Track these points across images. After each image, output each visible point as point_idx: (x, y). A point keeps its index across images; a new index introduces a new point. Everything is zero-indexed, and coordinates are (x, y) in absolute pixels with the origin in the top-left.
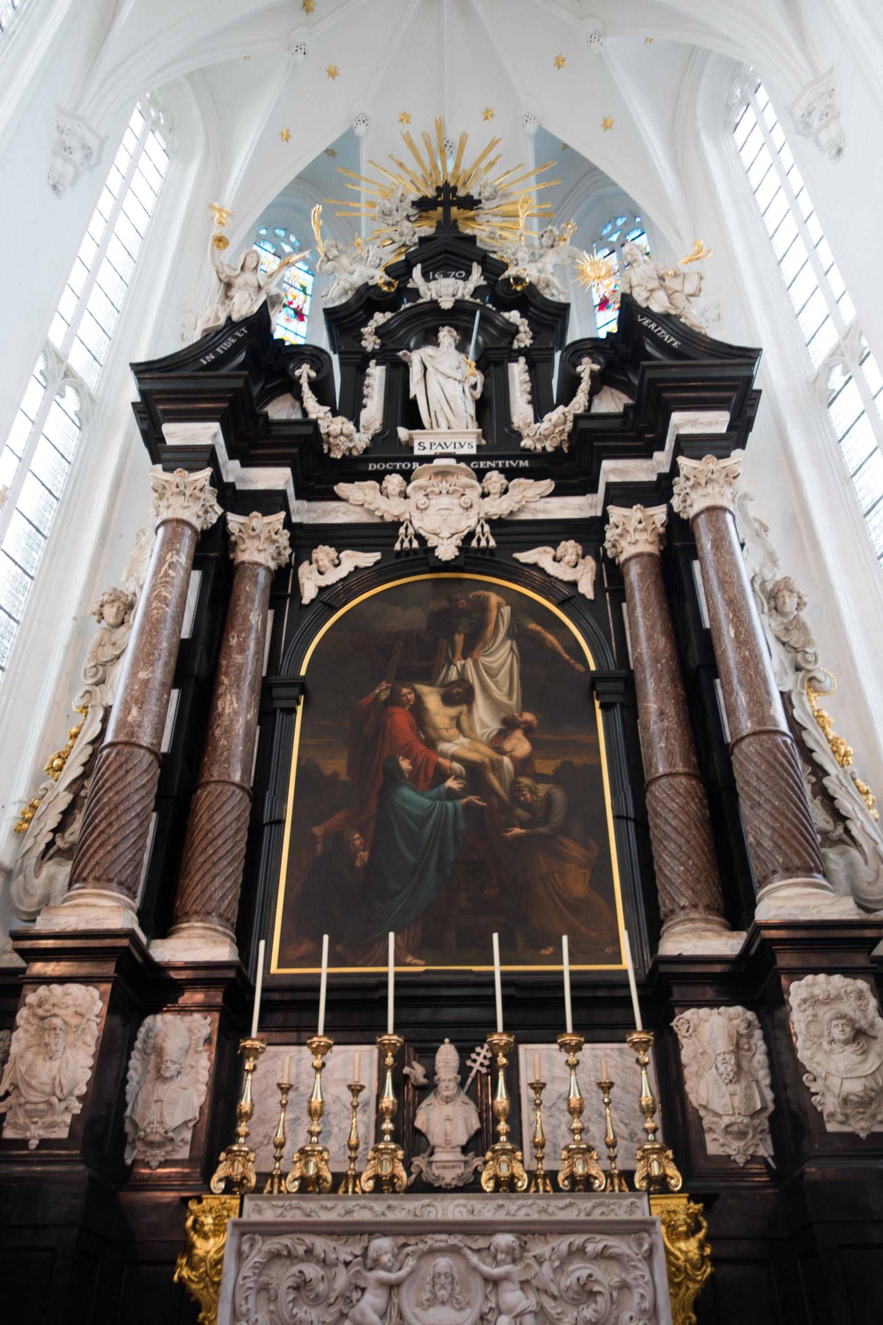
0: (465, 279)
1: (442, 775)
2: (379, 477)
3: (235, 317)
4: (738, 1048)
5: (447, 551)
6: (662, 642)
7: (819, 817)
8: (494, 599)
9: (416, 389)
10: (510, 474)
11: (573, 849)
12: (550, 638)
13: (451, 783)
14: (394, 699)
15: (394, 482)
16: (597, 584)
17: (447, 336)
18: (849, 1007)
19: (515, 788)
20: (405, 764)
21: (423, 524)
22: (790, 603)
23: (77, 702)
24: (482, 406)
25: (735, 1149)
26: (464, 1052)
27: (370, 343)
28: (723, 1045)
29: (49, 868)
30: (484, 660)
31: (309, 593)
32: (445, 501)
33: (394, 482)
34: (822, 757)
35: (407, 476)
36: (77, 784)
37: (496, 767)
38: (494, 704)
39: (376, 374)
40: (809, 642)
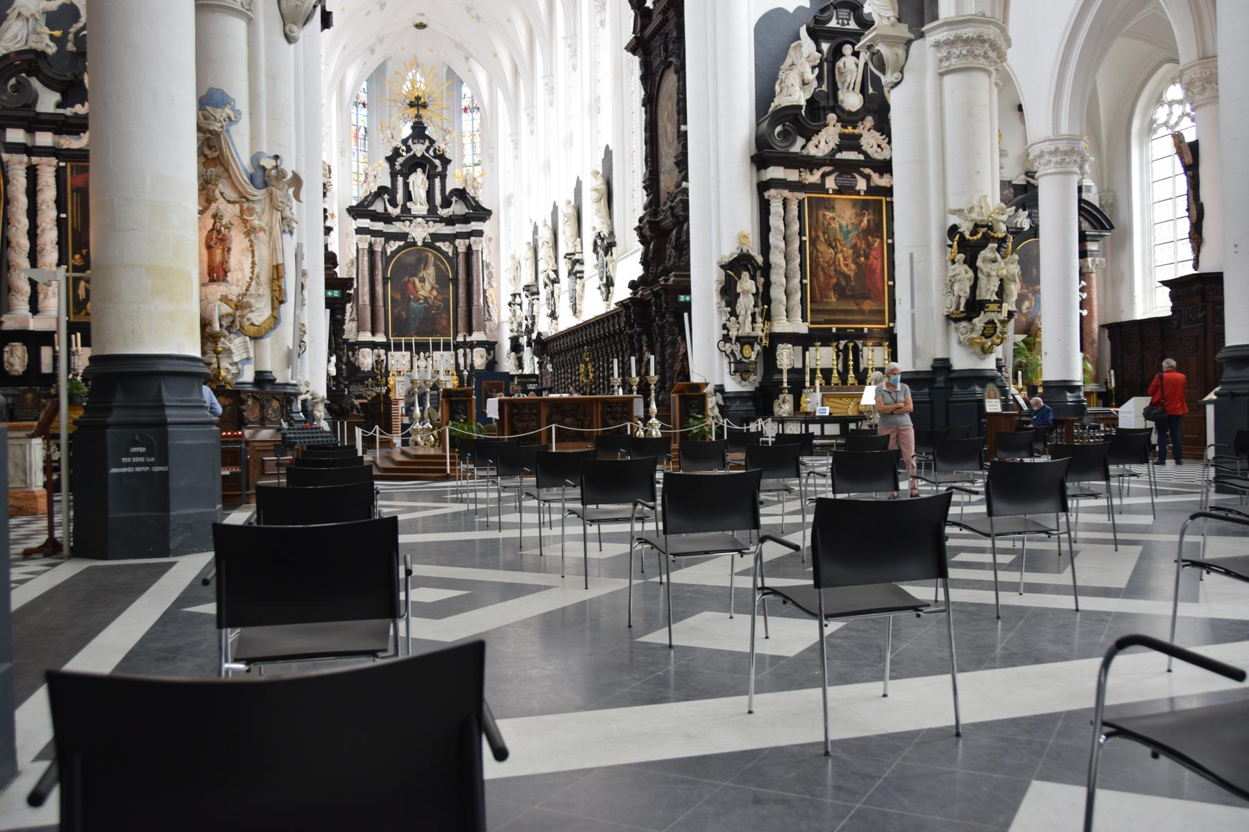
1: (419, 299)
2: (403, 221)
3: (373, 191)
5: (420, 243)
6: (464, 276)
7: (487, 316)
8: (430, 255)
9: (411, 188)
10: (435, 222)
11: (444, 316)
12: (442, 266)
13: (421, 301)
14: (409, 281)
15: (407, 223)
16: (453, 252)
17: (419, 170)
18: (481, 353)
20: (412, 297)
21: (413, 234)
22: (491, 268)
24: (428, 193)
27: (398, 167)
29: (351, 323)
30: (428, 272)
31: (389, 253)
32: (419, 229)
33: (407, 223)
34: (490, 304)
35: (411, 221)
37: (430, 298)
38: (430, 283)
39: (400, 179)
40: (492, 277)
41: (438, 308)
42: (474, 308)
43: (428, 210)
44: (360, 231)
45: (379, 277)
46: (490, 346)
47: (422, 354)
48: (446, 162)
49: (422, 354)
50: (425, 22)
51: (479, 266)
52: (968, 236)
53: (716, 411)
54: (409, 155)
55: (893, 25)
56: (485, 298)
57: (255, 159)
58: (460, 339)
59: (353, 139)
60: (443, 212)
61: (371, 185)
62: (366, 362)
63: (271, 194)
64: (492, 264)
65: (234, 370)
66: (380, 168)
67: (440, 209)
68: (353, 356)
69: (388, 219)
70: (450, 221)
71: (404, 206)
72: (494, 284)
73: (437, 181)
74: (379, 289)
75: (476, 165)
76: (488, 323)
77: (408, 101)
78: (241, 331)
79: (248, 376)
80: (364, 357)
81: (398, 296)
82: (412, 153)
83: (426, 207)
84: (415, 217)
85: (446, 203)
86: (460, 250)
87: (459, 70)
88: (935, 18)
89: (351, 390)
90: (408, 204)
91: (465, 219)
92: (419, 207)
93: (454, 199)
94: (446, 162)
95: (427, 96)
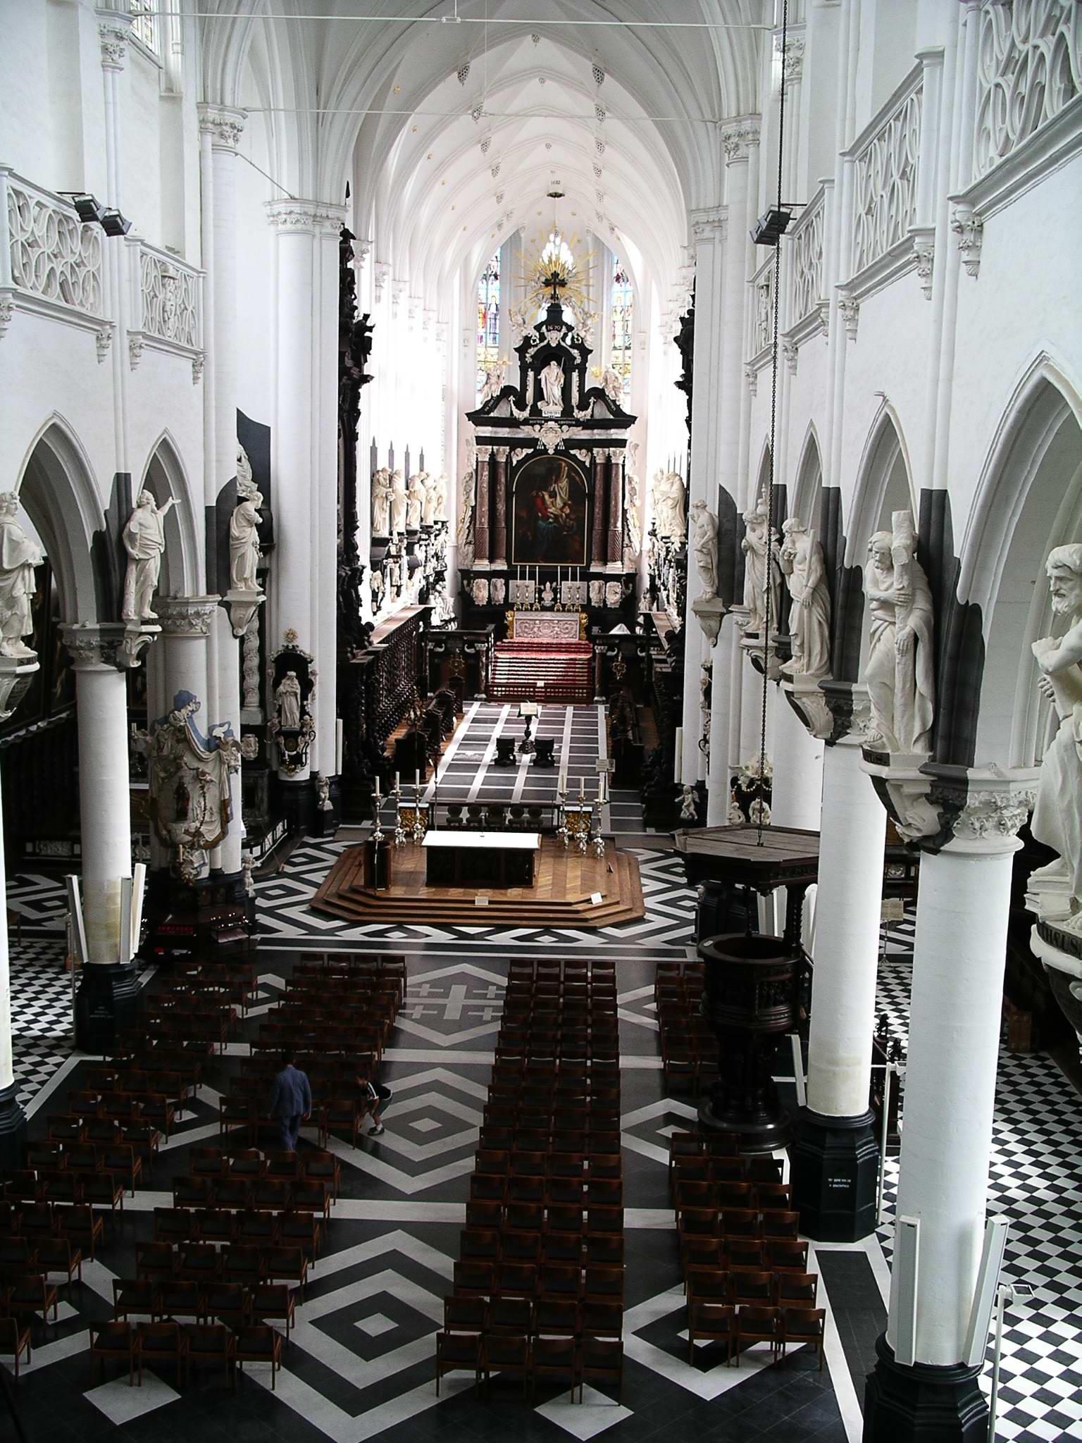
0: (560, 331)
2: (533, 425)
3: (495, 395)
4: (600, 588)
5: (551, 451)
10: (570, 426)
14: (537, 495)
15: (537, 427)
17: (553, 363)
19: (565, 522)
23: (463, 501)
24: (563, 390)
25: (596, 605)
26: (551, 584)
27: (529, 360)
28: (597, 588)
31: (515, 463)
32: (551, 435)
33: (537, 427)
36: (468, 528)
39: (531, 374)
41: (570, 528)
42: (610, 533)
43: (562, 412)
44: (481, 441)
45: (502, 493)
46: (630, 580)
47: (548, 584)
48: (585, 352)
49: (548, 584)
50: (561, 192)
51: (617, 482)
52: (744, 788)
53: (692, 808)
54: (542, 344)
55: (708, 601)
56: (625, 519)
57: (211, 729)
58: (595, 568)
59: (480, 321)
60: (578, 414)
61: (493, 388)
62: (481, 594)
63: (219, 754)
64: (636, 479)
65: (194, 872)
66: (504, 367)
67: (576, 411)
68: (469, 584)
69: (512, 423)
70: (589, 424)
71: (534, 406)
72: (637, 503)
73: (575, 375)
74: (501, 507)
75: (628, 348)
76: (626, 549)
77: (543, 279)
78: (200, 847)
79: (205, 873)
80: (479, 588)
81: (524, 514)
82: (546, 342)
83: (560, 409)
84: (547, 420)
85: (583, 406)
86: (598, 461)
87: (604, 235)
88: (741, 603)
89: (449, 646)
90: (539, 404)
91: (604, 424)
92: (552, 408)
93: (592, 400)
94: (585, 352)
95: (566, 272)
